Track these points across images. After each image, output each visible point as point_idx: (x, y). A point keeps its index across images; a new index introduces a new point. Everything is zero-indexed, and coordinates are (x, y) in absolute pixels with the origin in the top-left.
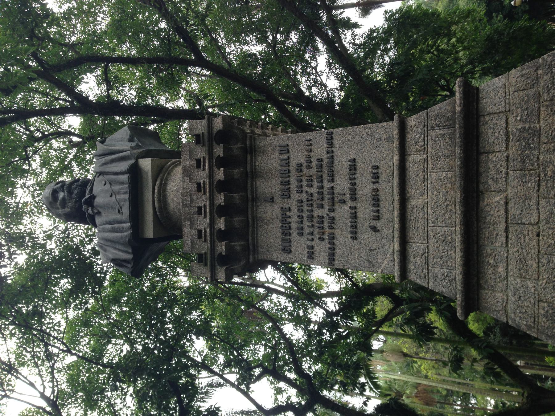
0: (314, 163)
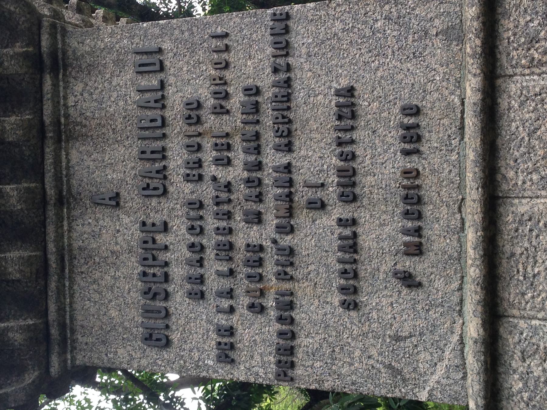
0: (237, 99)
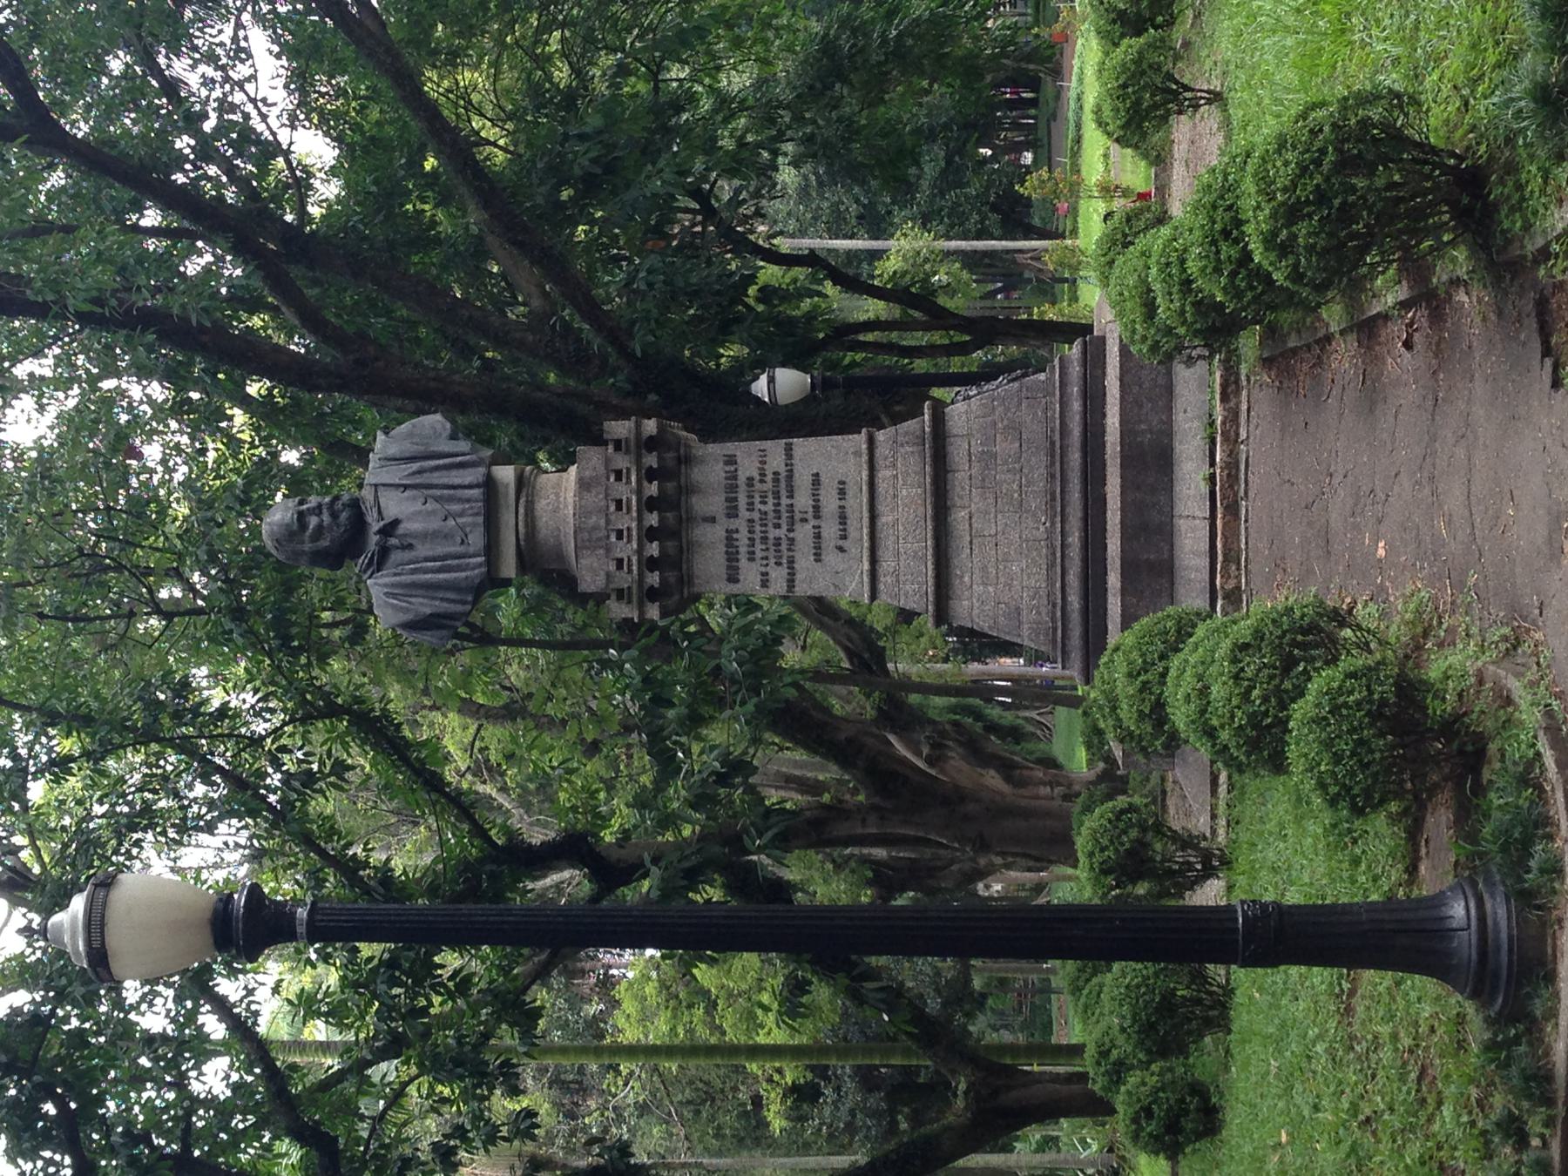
0: (769, 477)
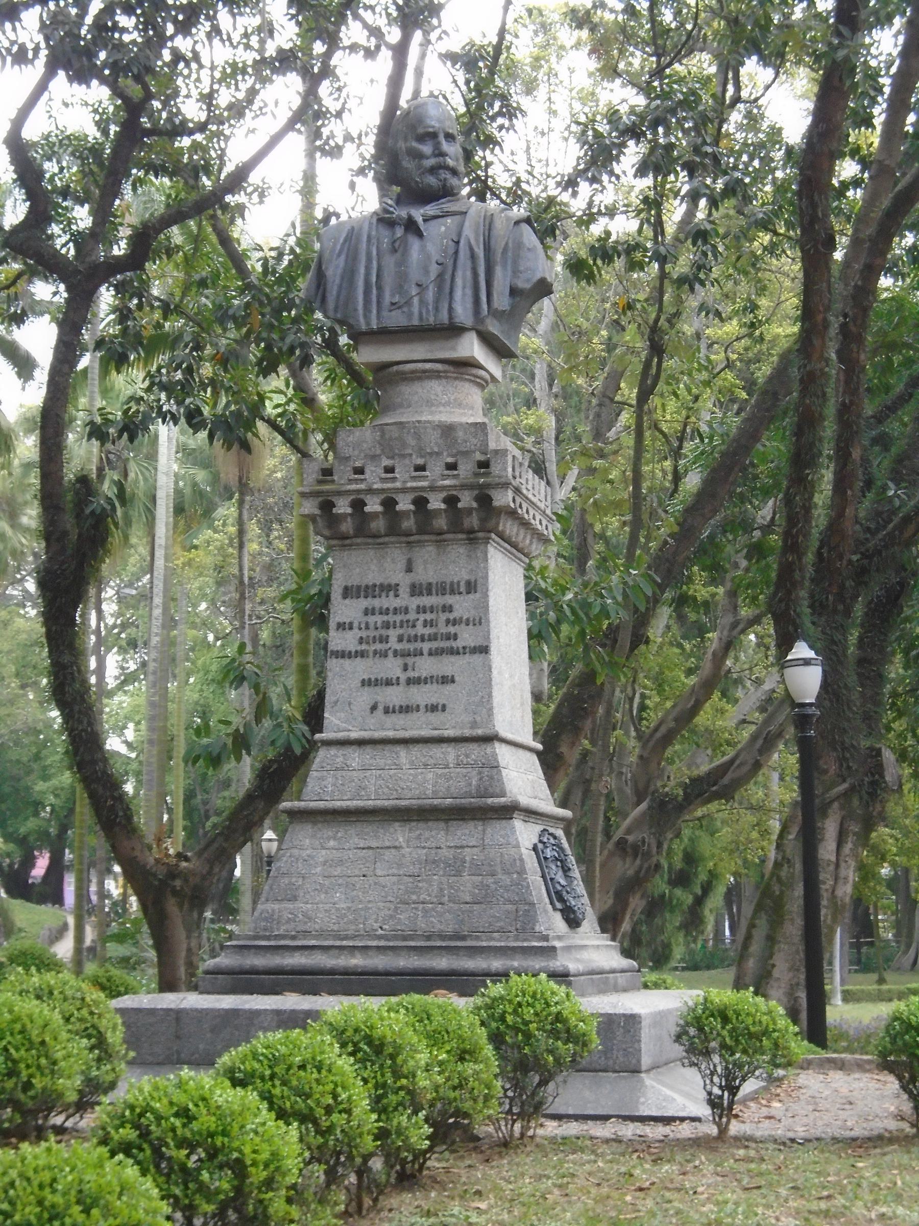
0: (452, 629)
